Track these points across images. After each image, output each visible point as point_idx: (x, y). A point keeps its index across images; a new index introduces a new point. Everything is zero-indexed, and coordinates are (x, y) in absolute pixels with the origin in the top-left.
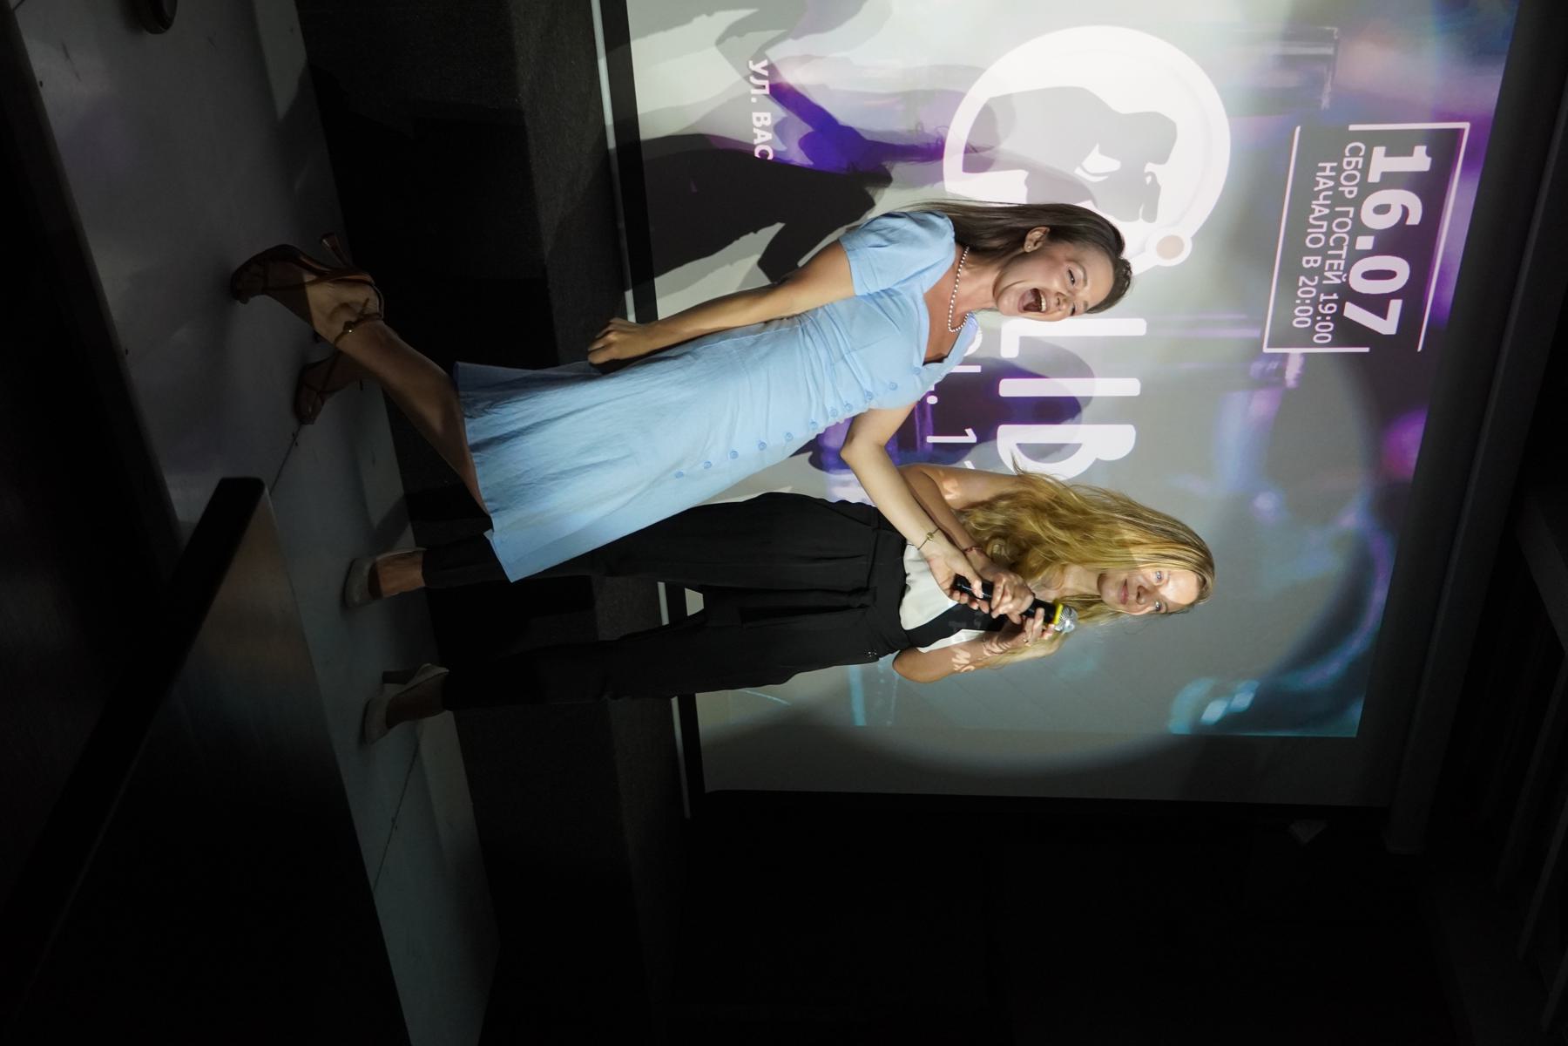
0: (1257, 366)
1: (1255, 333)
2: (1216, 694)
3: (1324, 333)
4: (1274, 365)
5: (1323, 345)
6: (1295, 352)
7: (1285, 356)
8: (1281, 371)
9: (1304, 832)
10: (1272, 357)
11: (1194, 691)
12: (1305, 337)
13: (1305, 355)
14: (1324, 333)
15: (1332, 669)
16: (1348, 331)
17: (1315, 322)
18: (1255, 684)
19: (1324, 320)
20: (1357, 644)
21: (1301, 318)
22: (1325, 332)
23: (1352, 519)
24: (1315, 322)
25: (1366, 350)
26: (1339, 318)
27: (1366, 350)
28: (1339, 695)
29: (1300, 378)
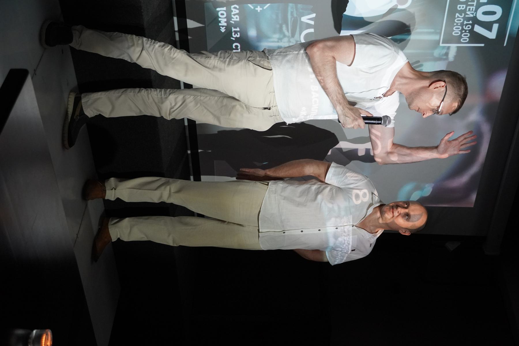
0: (437, 53)
1: (436, 37)
2: (417, 188)
3: (465, 38)
4: (444, 51)
5: (465, 43)
6: (454, 47)
7: (449, 48)
8: (447, 54)
9: (451, 246)
10: (444, 47)
11: (408, 188)
12: (458, 40)
13: (458, 47)
14: (465, 38)
15: (464, 179)
16: (475, 37)
17: (462, 33)
18: (433, 185)
19: (465, 32)
20: (475, 169)
21: (456, 31)
22: (466, 37)
23: (475, 116)
24: (462, 33)
25: (483, 45)
26: (472, 31)
27: (483, 45)
28: (467, 189)
29: (456, 57)
